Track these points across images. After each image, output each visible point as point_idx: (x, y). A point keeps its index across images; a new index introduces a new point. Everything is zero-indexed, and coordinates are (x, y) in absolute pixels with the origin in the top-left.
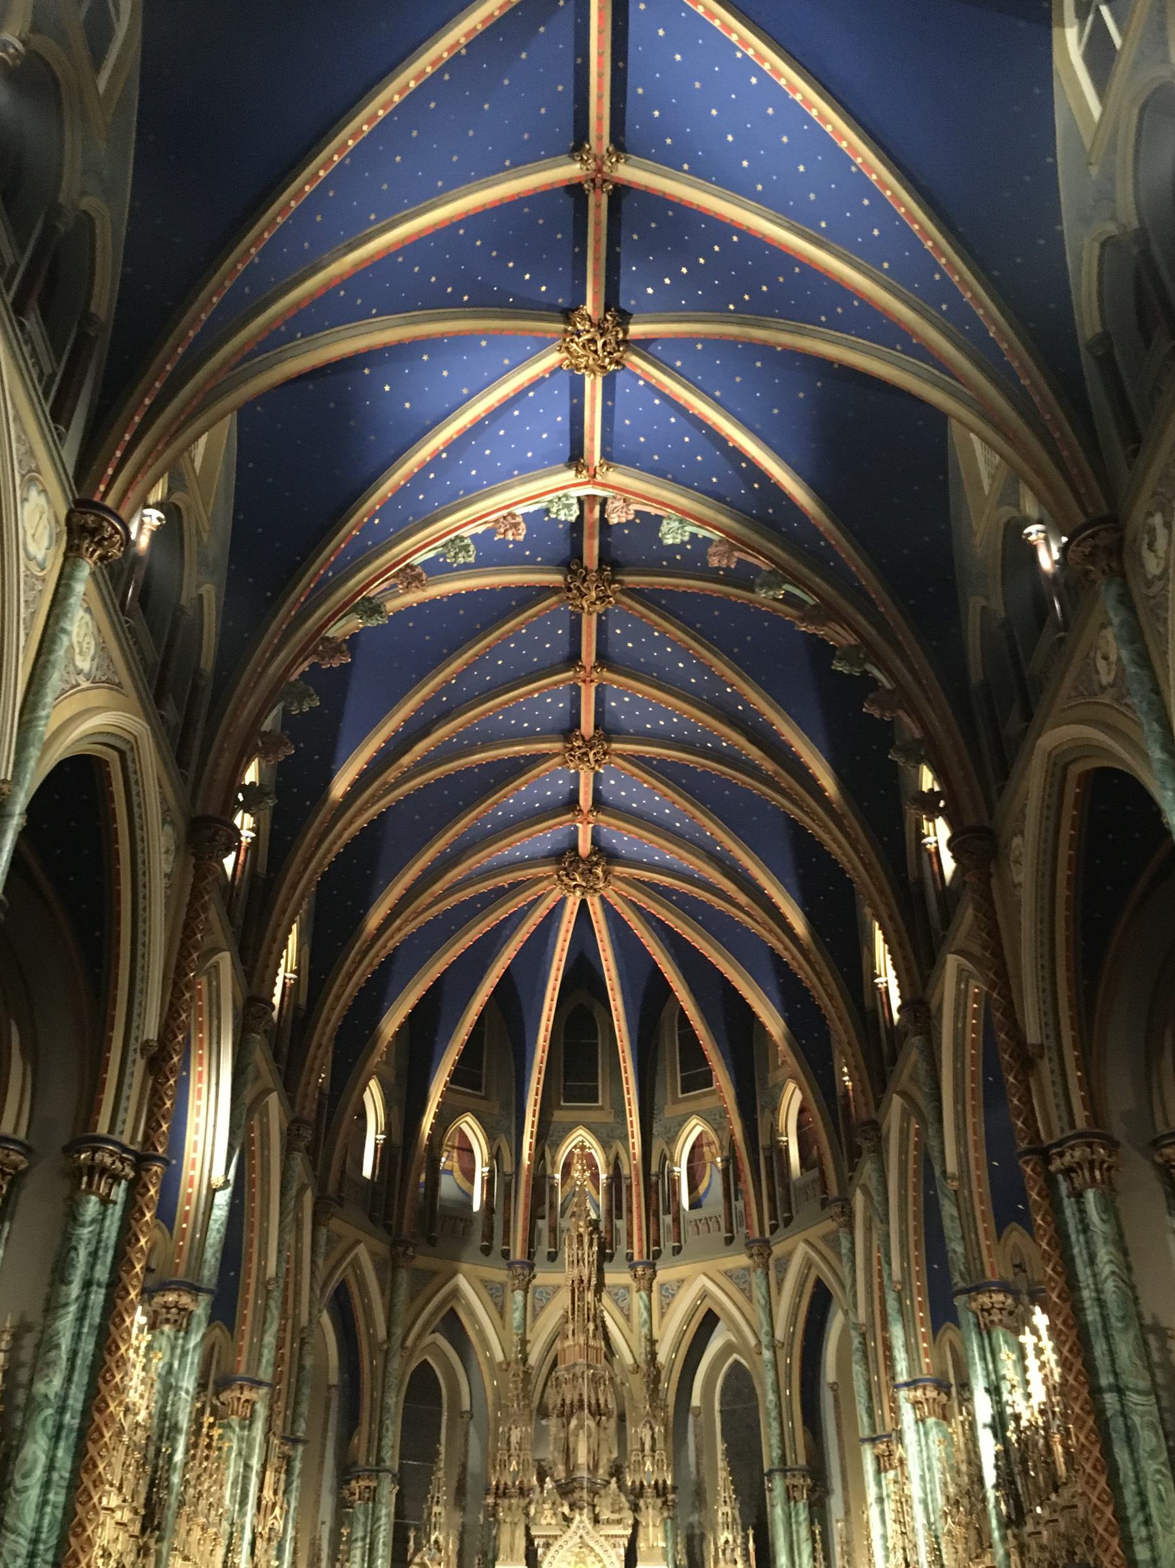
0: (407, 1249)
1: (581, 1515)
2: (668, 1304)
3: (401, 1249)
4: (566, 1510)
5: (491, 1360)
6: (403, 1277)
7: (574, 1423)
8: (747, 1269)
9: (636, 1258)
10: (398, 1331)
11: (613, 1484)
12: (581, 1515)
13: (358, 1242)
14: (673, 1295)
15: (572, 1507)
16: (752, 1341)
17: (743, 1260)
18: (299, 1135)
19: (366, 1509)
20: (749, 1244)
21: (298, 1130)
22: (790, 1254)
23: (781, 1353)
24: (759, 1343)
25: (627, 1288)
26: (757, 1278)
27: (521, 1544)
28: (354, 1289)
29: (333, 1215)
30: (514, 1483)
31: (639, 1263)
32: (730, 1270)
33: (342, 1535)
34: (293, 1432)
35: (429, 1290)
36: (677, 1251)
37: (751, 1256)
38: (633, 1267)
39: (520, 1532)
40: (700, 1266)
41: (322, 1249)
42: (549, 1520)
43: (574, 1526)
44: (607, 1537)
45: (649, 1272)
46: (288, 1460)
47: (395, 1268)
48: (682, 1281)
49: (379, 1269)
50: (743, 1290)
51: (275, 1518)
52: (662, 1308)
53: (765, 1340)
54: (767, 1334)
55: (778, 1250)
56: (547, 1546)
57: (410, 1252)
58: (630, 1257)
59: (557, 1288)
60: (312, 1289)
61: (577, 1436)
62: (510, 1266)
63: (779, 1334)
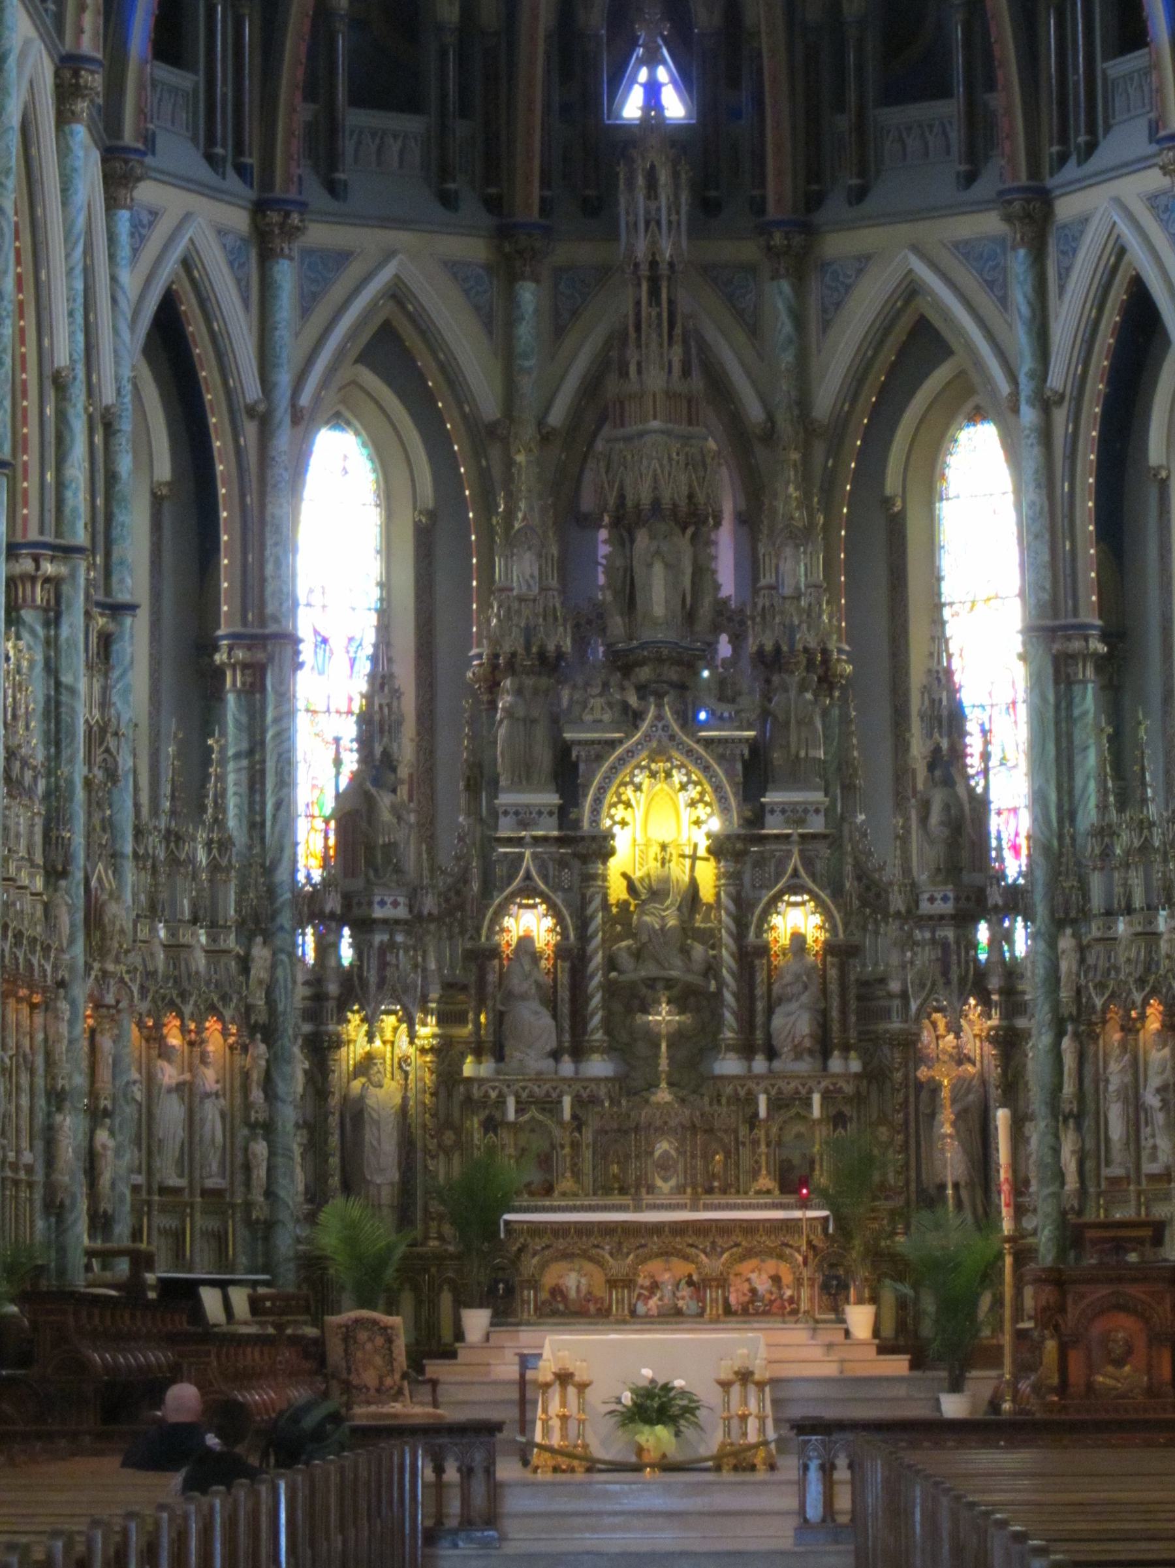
0: (287, 215)
1: (660, 706)
2: (838, 305)
3: (274, 217)
4: (633, 700)
5: (471, 422)
6: (286, 274)
7: (642, 539)
8: (1001, 241)
9: (772, 212)
10: (284, 378)
11: (724, 648)
12: (660, 706)
13: (187, 217)
14: (848, 288)
15: (642, 690)
16: (1005, 388)
17: (990, 223)
18: (77, 85)
20: (1002, 199)
21: (76, 74)
22: (1085, 220)
23: (1060, 416)
24: (1015, 395)
25: (751, 269)
26: (1018, 262)
27: (544, 756)
28: (188, 306)
29: (139, 179)
30: (528, 648)
31: (778, 224)
32: (967, 242)
33: (210, 750)
34: (108, 591)
35: (337, 292)
36: (859, 195)
37: (1008, 219)
38: (764, 230)
39: (541, 733)
40: (904, 231)
41: (124, 252)
42: (597, 715)
43: (644, 726)
44: (708, 743)
45: (798, 240)
46: (106, 641)
47: (266, 256)
48: (864, 261)
49: (235, 262)
50: (990, 284)
51: (107, 750)
52: (825, 311)
53: (1026, 387)
54: (1032, 375)
55: (1066, 208)
56: (599, 758)
57: (295, 219)
58: (758, 207)
59: (604, 272)
60: (116, 331)
61: (650, 566)
62: (504, 233)
63: (1056, 380)
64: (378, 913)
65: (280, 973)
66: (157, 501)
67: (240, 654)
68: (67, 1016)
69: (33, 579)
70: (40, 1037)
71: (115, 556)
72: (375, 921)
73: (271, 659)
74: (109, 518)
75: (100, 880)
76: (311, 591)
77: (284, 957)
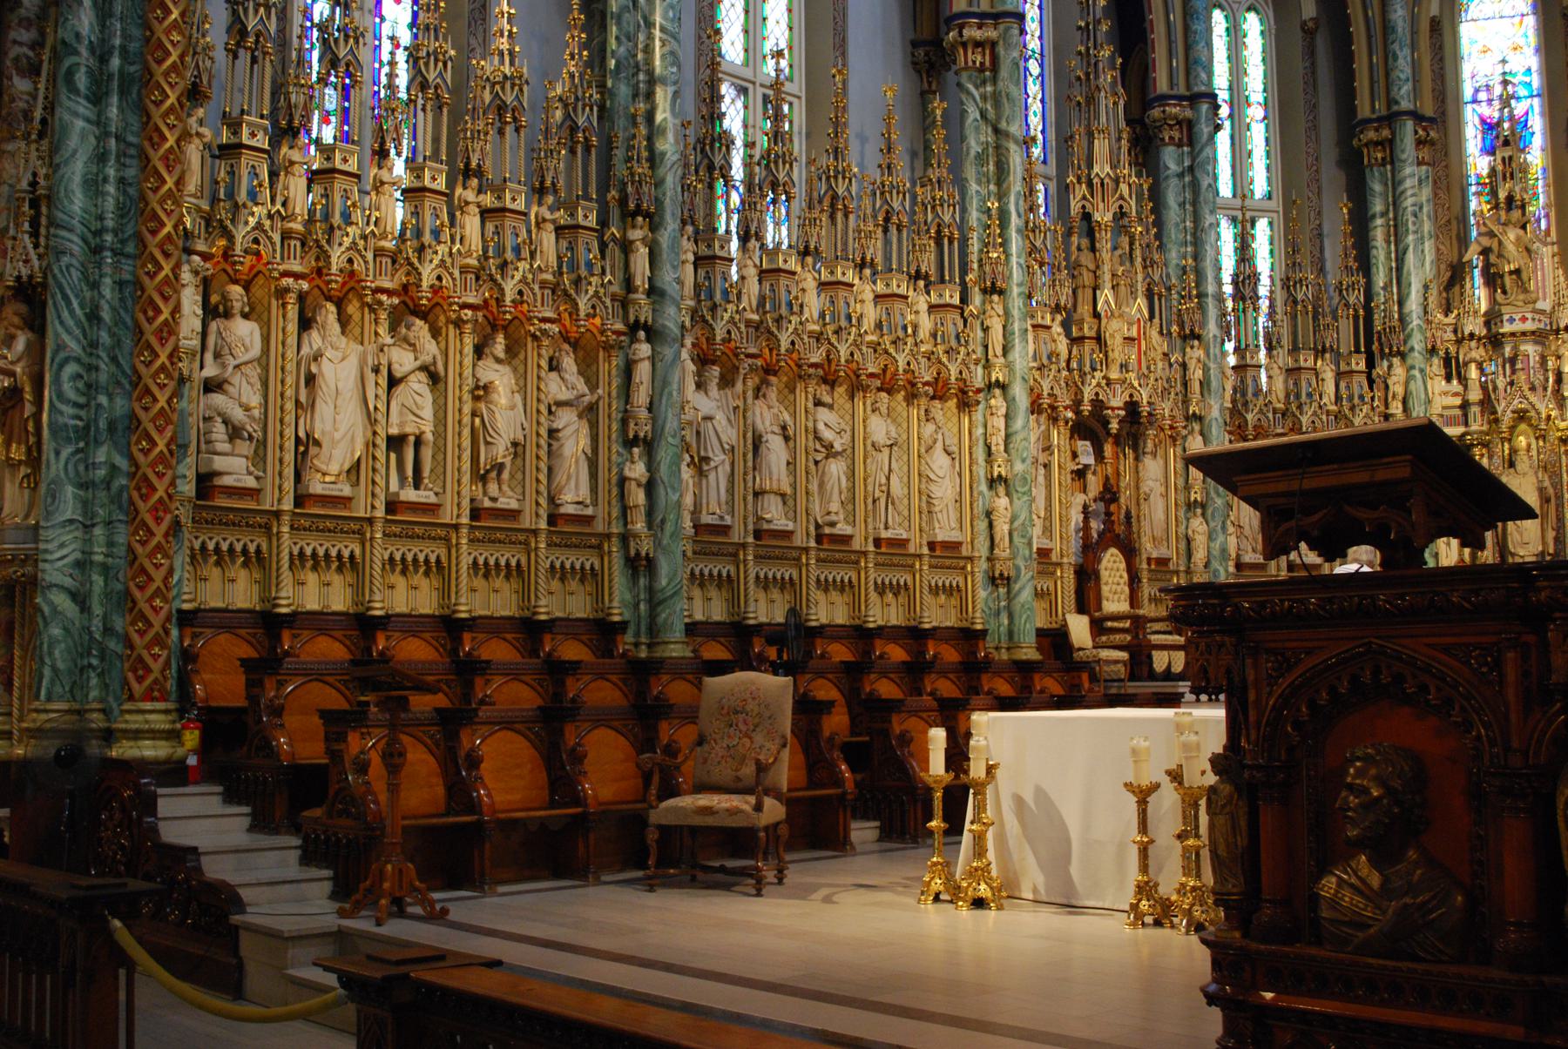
19: (1384, 175)
51: (1122, 198)
64: (1507, 328)
65: (1412, 386)
66: (1309, 32)
67: (1372, 135)
68: (1003, 411)
69: (964, 45)
70: (980, 431)
71: (1191, 58)
72: (1503, 335)
73: (1393, 133)
74: (1187, 29)
75: (1107, 302)
76: (1477, 91)
77: (1416, 373)
